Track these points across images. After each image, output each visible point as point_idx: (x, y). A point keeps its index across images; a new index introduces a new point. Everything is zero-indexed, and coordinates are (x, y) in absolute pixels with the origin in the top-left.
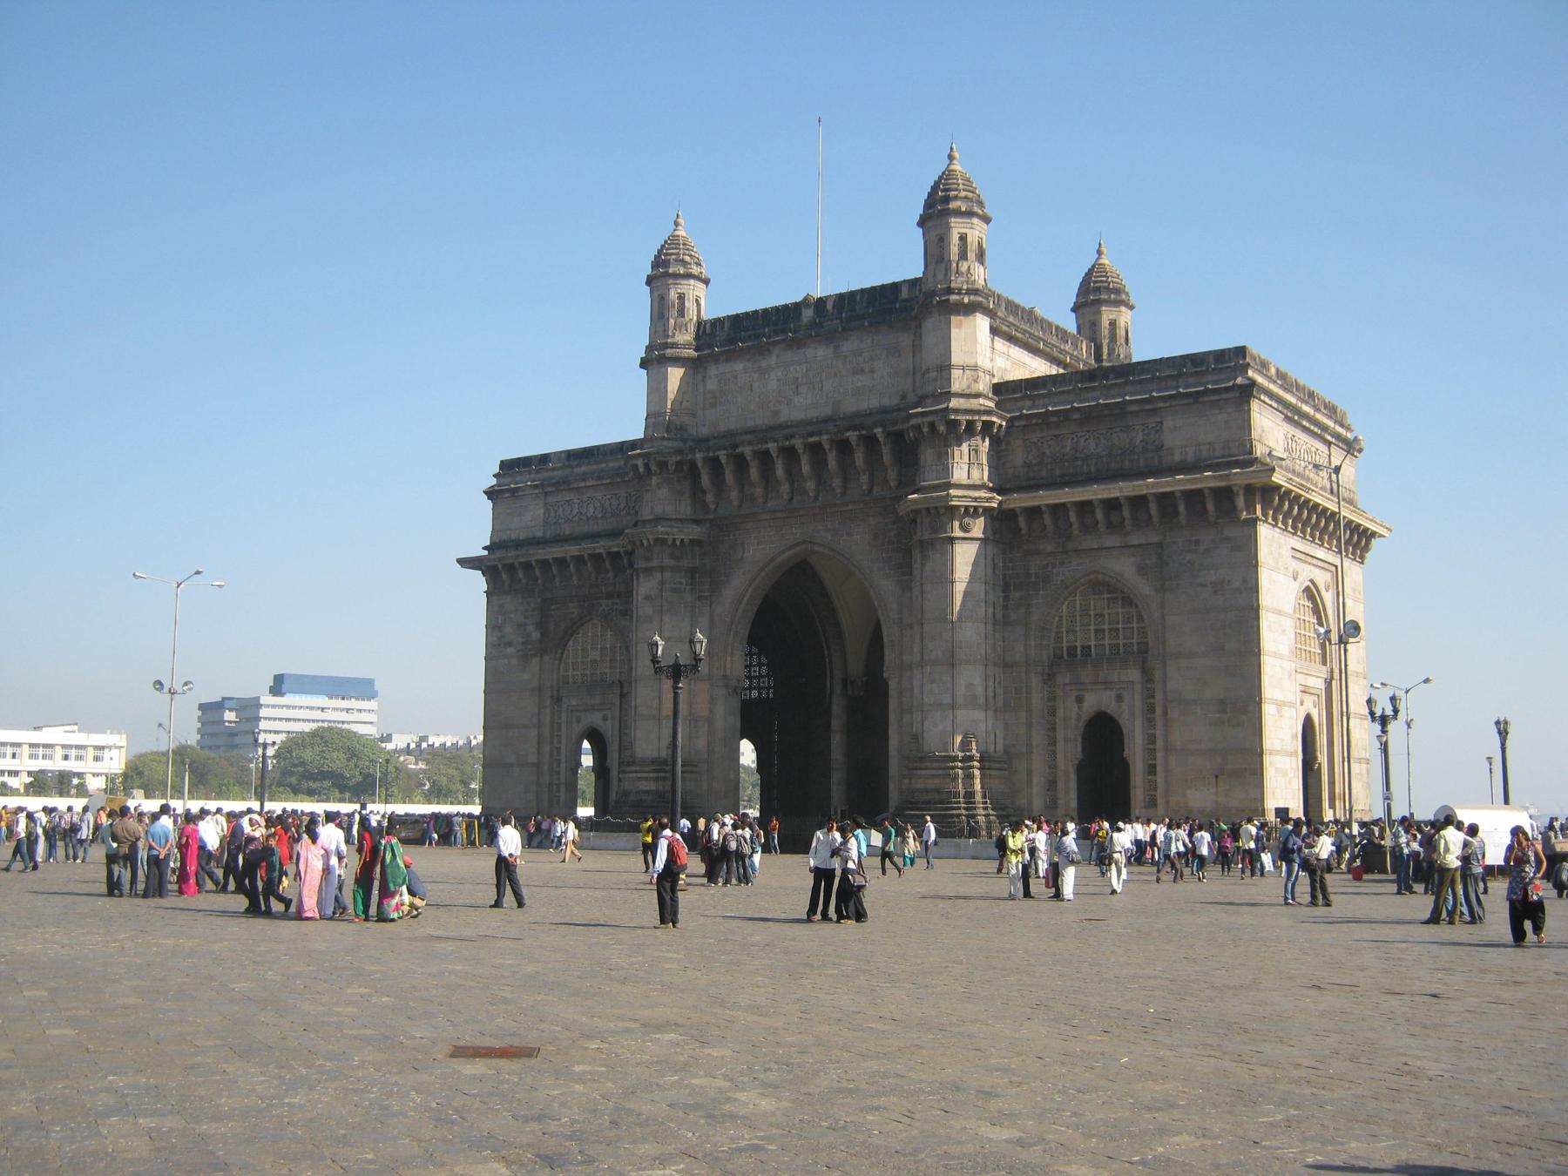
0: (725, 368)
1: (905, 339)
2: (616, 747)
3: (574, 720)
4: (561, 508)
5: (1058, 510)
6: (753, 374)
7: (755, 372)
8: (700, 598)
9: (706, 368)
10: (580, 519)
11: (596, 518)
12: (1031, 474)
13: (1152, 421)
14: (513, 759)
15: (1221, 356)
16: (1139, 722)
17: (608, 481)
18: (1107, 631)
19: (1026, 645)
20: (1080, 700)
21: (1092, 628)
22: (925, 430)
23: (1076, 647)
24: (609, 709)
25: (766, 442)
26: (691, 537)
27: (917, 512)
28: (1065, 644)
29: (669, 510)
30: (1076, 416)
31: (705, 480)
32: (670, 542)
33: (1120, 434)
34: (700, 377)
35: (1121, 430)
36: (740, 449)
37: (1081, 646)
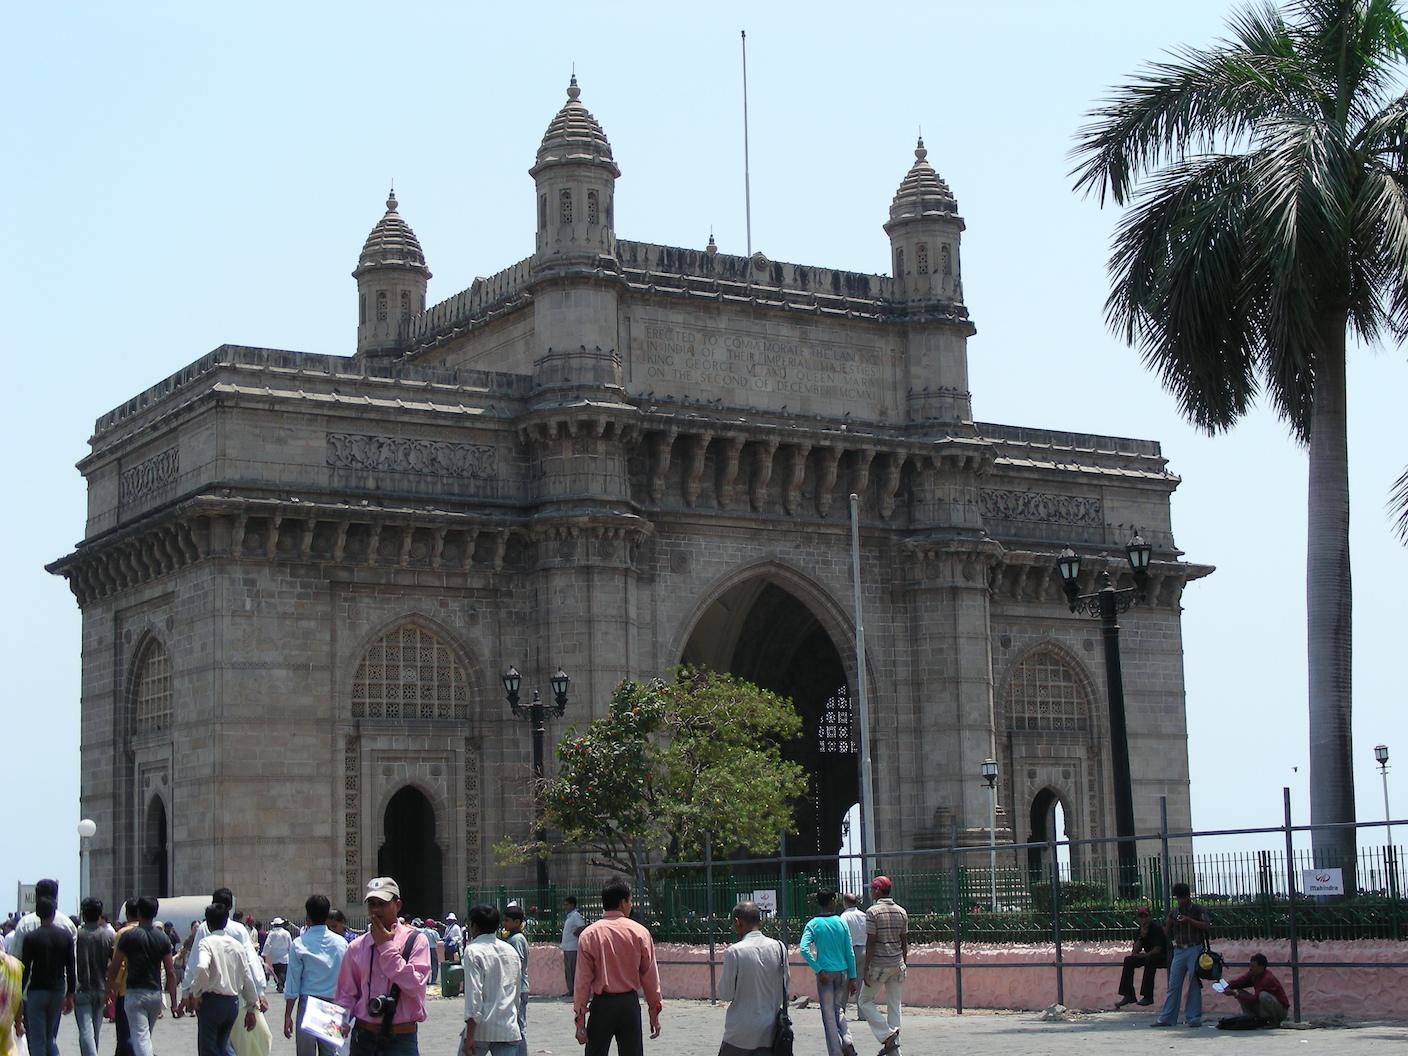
1: (885, 346)
2: (462, 810)
3: (381, 770)
6: (695, 333)
7: (699, 331)
10: (393, 471)
11: (419, 473)
13: (1093, 496)
14: (284, 830)
15: (1142, 444)
16: (1086, 799)
20: (1032, 775)
21: (1039, 699)
22: (962, 464)
23: (1023, 718)
24: (447, 759)
28: (1014, 715)
36: (731, 434)
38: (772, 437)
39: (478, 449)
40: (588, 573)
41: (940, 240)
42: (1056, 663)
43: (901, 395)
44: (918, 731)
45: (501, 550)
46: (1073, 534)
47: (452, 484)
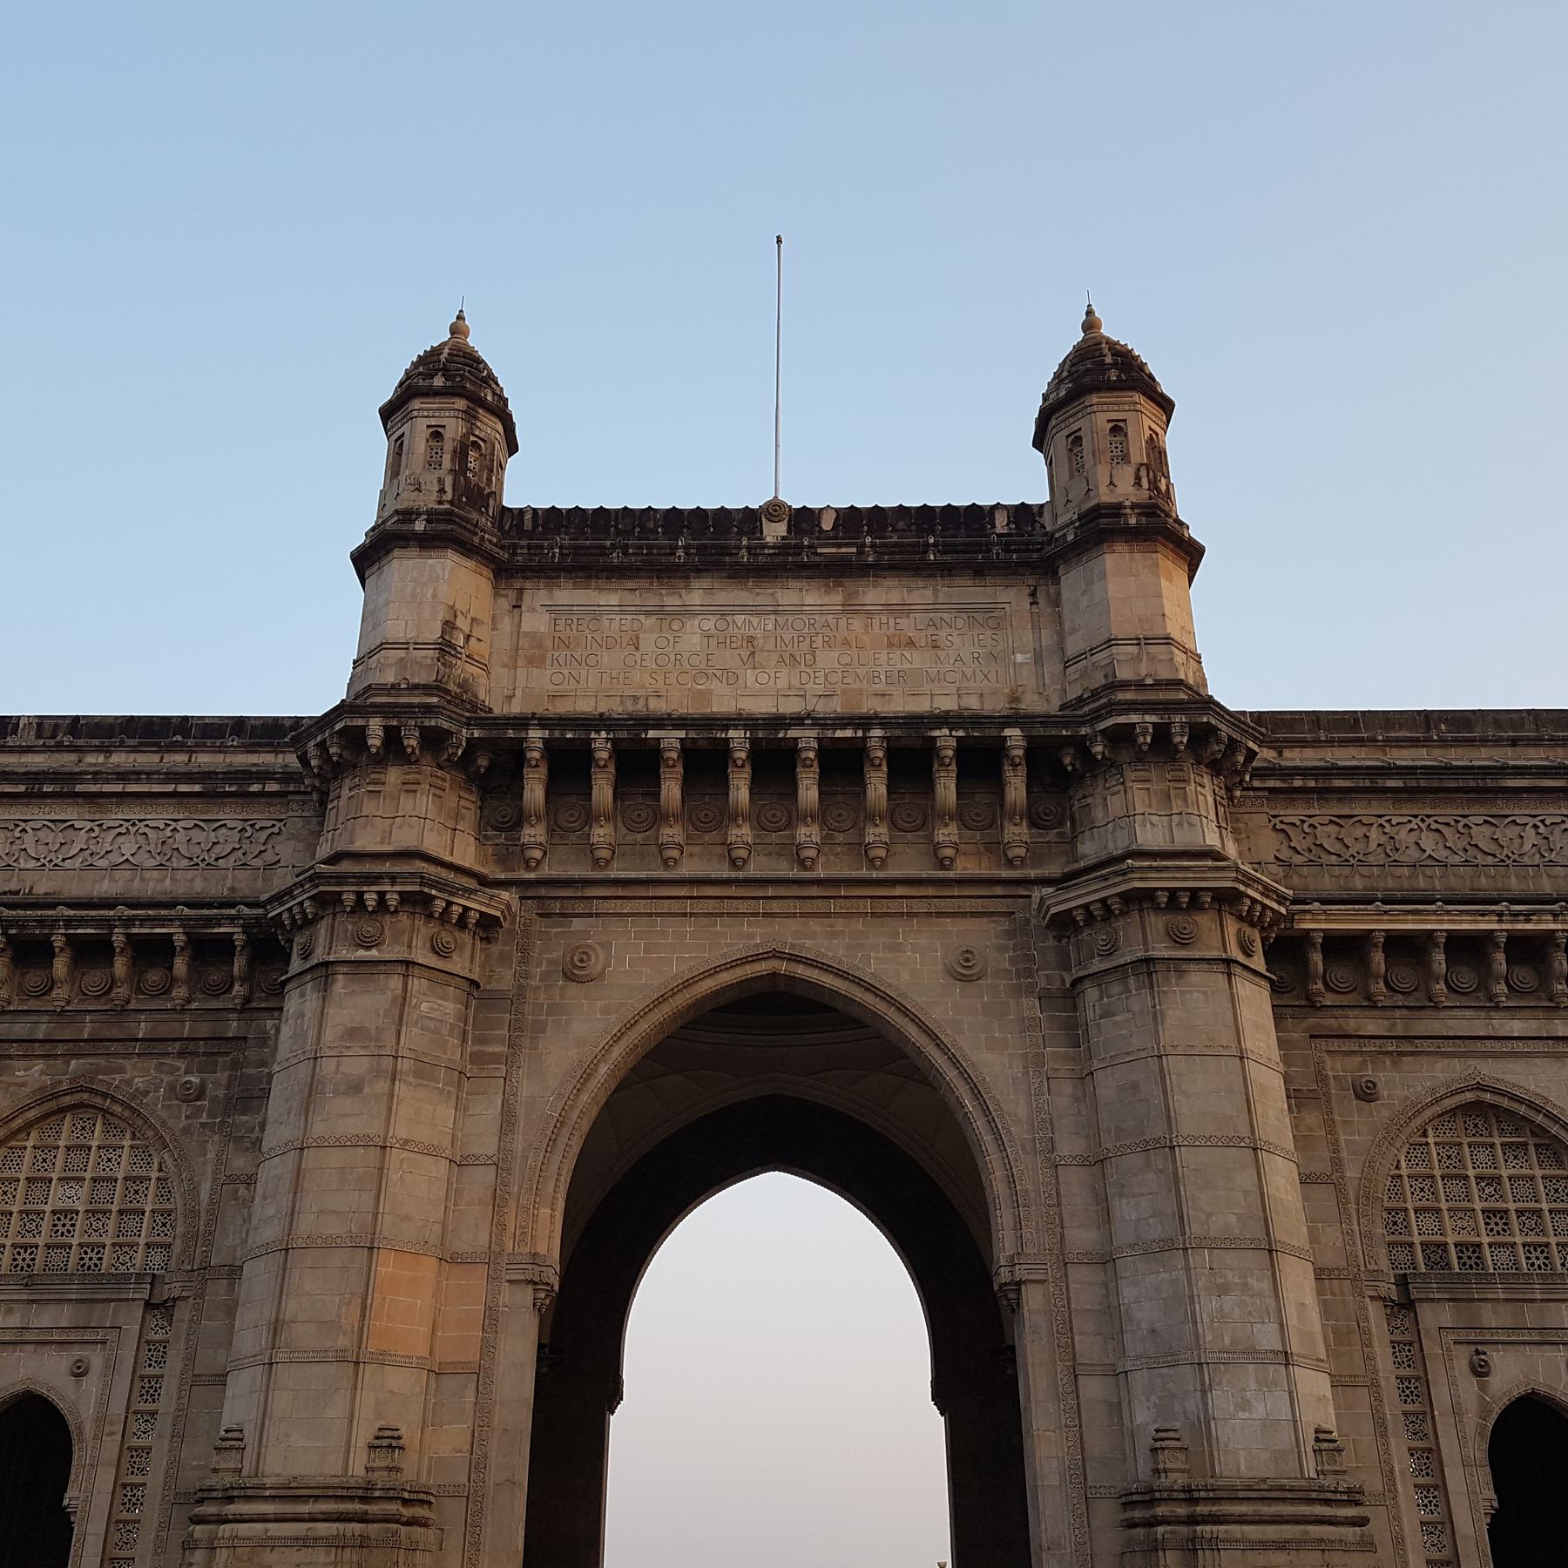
0: (566, 594)
4: (29, 839)
5: (1407, 947)
6: (642, 618)
7: (648, 613)
8: (477, 1059)
9: (521, 591)
11: (135, 868)
12: (1296, 880)
17: (197, 788)
18: (1514, 1216)
19: (1342, 1233)
21: (1478, 1206)
23: (1446, 1244)
25: (726, 728)
26: (484, 909)
27: (1141, 899)
29: (433, 843)
30: (1391, 783)
31: (534, 791)
32: (439, 905)
33: (1487, 829)
34: (505, 604)
35: (1486, 822)
36: (652, 734)
37: (1456, 1245)
38: (732, 733)
39: (252, 826)
40: (327, 976)
41: (1102, 420)
42: (1517, 1131)
43: (1052, 668)
44: (1106, 1261)
45: (239, 964)
46: (1513, 879)
47: (192, 880)
